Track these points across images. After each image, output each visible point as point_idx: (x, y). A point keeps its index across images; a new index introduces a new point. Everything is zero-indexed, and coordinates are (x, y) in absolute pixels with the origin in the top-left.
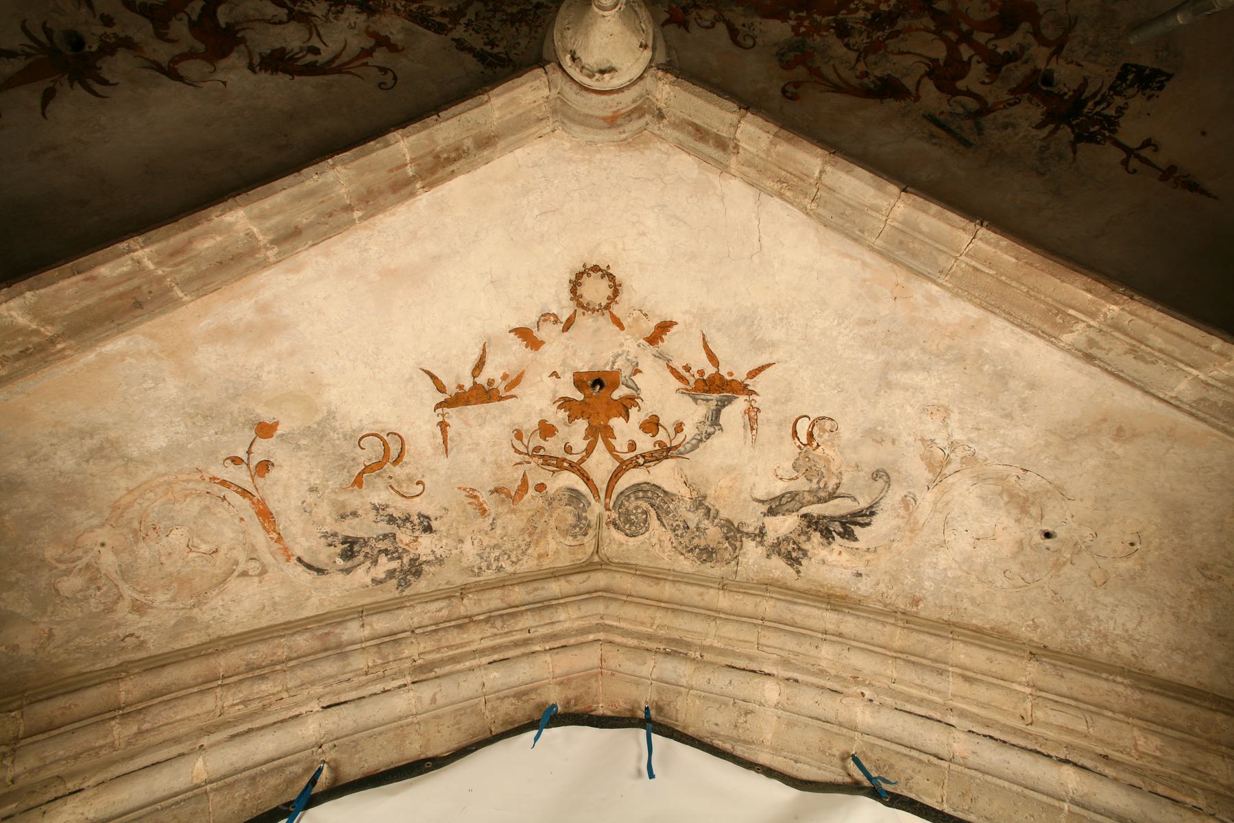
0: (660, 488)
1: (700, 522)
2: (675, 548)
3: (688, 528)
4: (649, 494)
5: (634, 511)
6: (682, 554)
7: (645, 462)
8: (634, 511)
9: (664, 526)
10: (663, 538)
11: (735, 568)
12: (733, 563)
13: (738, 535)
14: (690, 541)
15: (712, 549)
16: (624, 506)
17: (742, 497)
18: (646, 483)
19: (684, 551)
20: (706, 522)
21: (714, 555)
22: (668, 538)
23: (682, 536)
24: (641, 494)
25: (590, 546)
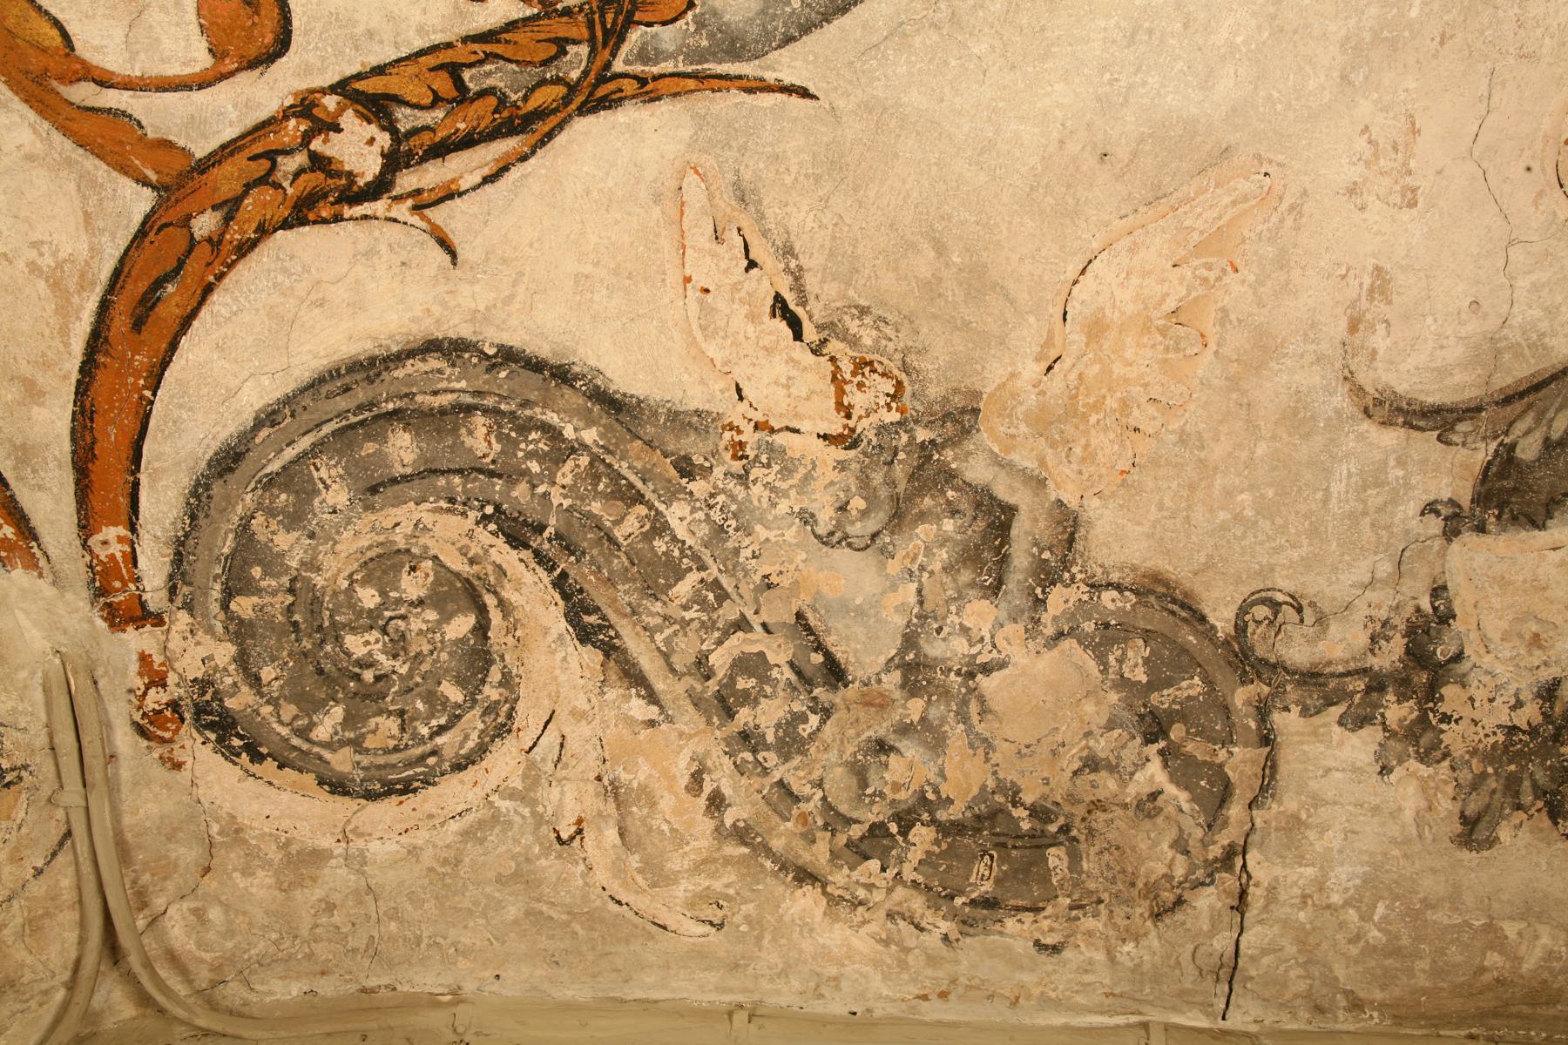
0: (562, 375)
1: (924, 618)
2: (741, 834)
3: (835, 672)
4: (479, 439)
5: (368, 597)
6: (805, 876)
7: (394, 162)
8: (368, 597)
9: (635, 678)
10: (637, 774)
11: (1222, 943)
12: (1207, 901)
13: (1241, 697)
14: (860, 775)
15: (1039, 813)
16: (273, 562)
17: (1271, 390)
18: (432, 346)
19: (818, 854)
20: (980, 614)
21: (1056, 858)
22: (682, 769)
23: (791, 742)
24: (402, 448)
25: (33, 927)
